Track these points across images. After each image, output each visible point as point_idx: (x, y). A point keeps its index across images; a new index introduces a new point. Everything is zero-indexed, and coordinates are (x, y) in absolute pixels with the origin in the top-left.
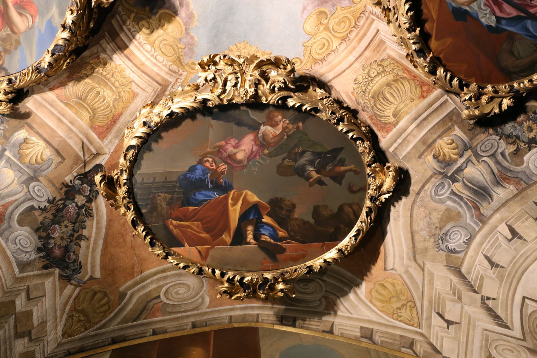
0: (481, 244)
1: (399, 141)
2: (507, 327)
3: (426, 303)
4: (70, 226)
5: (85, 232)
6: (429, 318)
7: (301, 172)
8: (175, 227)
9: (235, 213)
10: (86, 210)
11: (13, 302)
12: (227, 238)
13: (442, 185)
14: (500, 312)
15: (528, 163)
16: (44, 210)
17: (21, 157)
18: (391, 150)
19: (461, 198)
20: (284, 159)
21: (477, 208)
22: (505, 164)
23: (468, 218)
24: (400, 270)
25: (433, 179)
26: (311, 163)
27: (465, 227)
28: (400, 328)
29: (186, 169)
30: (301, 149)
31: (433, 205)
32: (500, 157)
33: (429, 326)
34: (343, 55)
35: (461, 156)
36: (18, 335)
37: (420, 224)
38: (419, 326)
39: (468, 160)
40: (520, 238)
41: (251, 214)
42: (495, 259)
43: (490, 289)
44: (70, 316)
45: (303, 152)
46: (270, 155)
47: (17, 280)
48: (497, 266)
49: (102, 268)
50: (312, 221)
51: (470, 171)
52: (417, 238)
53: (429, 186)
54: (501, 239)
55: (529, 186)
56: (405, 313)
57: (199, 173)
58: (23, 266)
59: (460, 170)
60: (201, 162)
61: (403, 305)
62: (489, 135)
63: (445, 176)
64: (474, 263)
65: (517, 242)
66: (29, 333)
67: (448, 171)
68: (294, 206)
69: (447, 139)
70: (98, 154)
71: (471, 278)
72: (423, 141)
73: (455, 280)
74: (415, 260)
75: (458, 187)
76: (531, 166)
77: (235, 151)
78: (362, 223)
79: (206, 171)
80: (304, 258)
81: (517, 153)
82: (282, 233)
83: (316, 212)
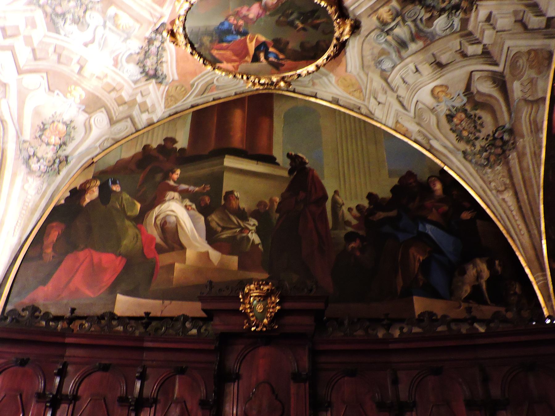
0: (400, 70)
4: (155, 58)
5: (164, 59)
6: (369, 98)
7: (291, 24)
8: (217, 54)
9: (252, 47)
10: (162, 48)
11: (135, 99)
12: (249, 59)
13: (380, 35)
14: (405, 103)
15: (436, 25)
16: (138, 53)
17: (117, 26)
18: (351, 8)
20: (280, 17)
22: (421, 26)
23: (394, 55)
24: (354, 73)
25: (376, 31)
26: (298, 18)
27: (392, 60)
28: (354, 100)
30: (290, 11)
31: (374, 44)
32: (418, 22)
33: (369, 102)
35: (394, 20)
36: (142, 112)
37: (367, 53)
38: (364, 100)
39: (397, 24)
40: (420, 73)
41: (261, 47)
42: (405, 79)
43: (402, 92)
44: (166, 99)
45: (292, 14)
46: (271, 15)
47: (134, 89)
48: (406, 83)
49: (178, 74)
50: (300, 50)
51: (398, 31)
52: (364, 59)
53: (373, 34)
55: (432, 42)
56: (357, 94)
57: (226, 26)
58: (135, 82)
59: (392, 29)
60: (227, 19)
62: (415, 5)
63: (382, 30)
64: (395, 78)
66: (148, 110)
68: (288, 43)
69: (386, 8)
70: (161, 17)
71: (393, 85)
72: (371, 7)
73: (384, 84)
75: (389, 38)
76: (437, 29)
77: (247, 13)
78: (331, 51)
79: (230, 25)
80: (296, 69)
81: (431, 19)
82: (281, 56)
83: (302, 45)
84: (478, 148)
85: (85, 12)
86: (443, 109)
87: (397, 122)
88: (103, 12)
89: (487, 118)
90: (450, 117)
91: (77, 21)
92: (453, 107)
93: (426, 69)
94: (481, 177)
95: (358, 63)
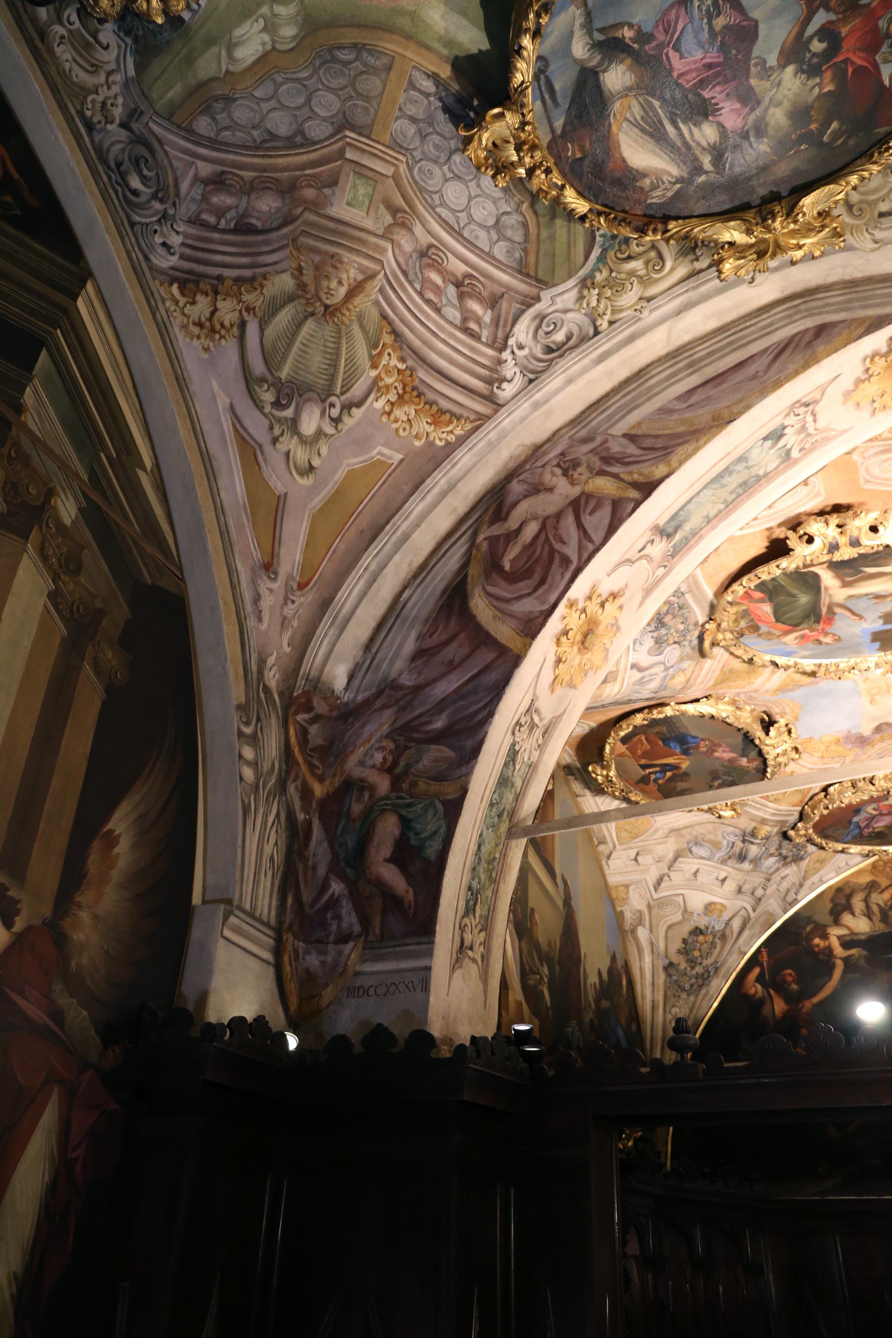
1: (758, 806)
2: (656, 890)
3: (641, 844)
19: (732, 847)
21: (730, 858)
24: (657, 825)
29: (693, 734)
34: (810, 760)
37: (700, 830)
40: (722, 884)
52: (689, 830)
53: (731, 829)
54: (715, 875)
59: (752, 843)
60: (703, 740)
61: (631, 832)
64: (688, 865)
65: (719, 883)
67: (749, 836)
71: (677, 864)
73: (671, 856)
74: (671, 832)
75: (741, 845)
84: (694, 972)
85: (675, 643)
86: (702, 923)
87: (627, 887)
88: (681, 659)
89: (717, 951)
90: (697, 931)
91: (659, 642)
92: (713, 927)
93: (731, 886)
94: (665, 995)
95: (676, 825)
